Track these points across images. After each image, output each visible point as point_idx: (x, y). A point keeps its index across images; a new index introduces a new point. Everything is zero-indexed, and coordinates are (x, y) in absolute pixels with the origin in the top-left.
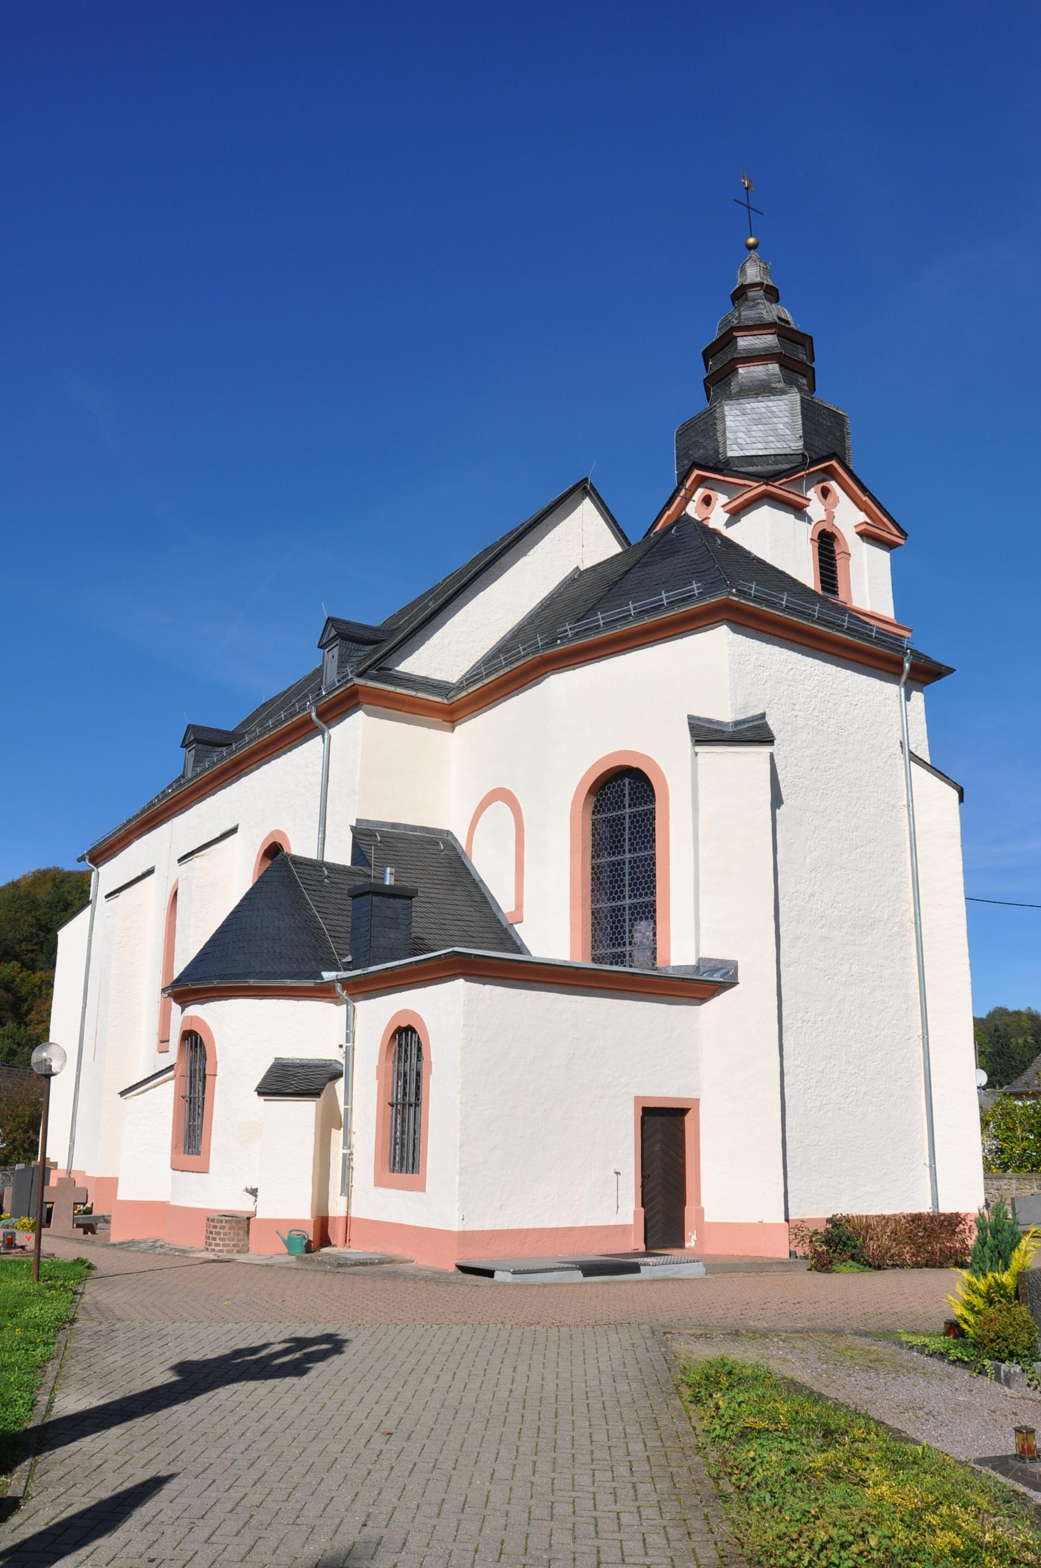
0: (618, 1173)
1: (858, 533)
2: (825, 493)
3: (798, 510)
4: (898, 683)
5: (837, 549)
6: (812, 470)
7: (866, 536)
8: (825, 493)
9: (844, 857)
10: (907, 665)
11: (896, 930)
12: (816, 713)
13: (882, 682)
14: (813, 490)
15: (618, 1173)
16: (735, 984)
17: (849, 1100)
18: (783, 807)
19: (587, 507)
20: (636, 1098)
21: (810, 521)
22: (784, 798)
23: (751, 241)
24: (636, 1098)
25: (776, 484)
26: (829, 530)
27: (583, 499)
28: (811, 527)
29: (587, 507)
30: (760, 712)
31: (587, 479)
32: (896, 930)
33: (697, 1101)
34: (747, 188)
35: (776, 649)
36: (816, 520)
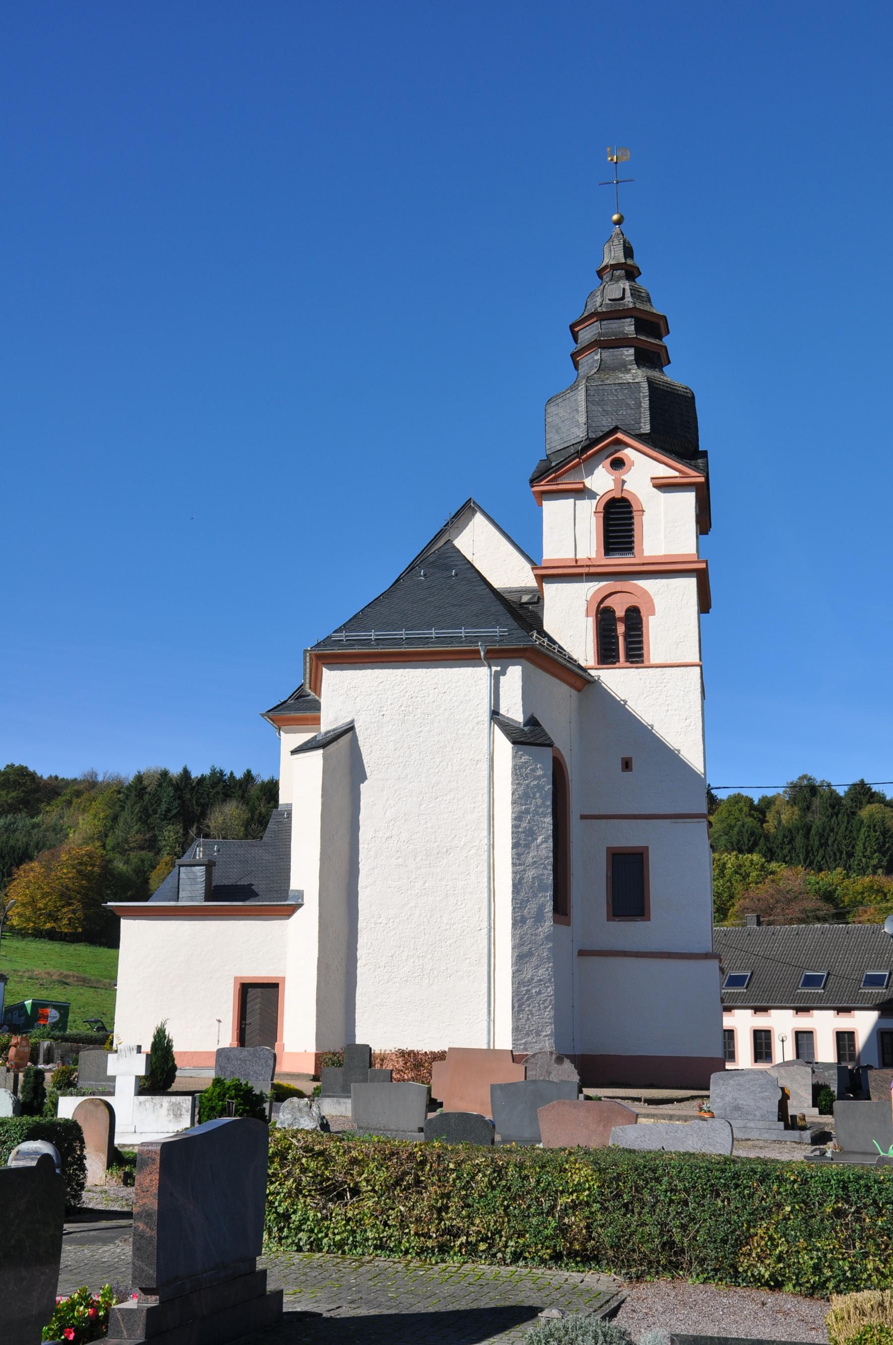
0: (219, 1021)
2: (618, 464)
3: (582, 493)
4: (484, 666)
5: (635, 508)
7: (664, 486)
8: (618, 464)
9: (423, 806)
10: (482, 653)
11: (473, 851)
12: (403, 708)
14: (601, 466)
15: (219, 1021)
16: (302, 905)
17: (416, 975)
18: (366, 782)
19: (479, 519)
20: (235, 978)
21: (591, 495)
22: (368, 775)
23: (615, 217)
24: (235, 978)
25: (542, 483)
26: (618, 496)
27: (473, 515)
28: (595, 502)
29: (479, 519)
30: (348, 720)
32: (473, 851)
33: (284, 979)
35: (369, 671)
36: (601, 492)
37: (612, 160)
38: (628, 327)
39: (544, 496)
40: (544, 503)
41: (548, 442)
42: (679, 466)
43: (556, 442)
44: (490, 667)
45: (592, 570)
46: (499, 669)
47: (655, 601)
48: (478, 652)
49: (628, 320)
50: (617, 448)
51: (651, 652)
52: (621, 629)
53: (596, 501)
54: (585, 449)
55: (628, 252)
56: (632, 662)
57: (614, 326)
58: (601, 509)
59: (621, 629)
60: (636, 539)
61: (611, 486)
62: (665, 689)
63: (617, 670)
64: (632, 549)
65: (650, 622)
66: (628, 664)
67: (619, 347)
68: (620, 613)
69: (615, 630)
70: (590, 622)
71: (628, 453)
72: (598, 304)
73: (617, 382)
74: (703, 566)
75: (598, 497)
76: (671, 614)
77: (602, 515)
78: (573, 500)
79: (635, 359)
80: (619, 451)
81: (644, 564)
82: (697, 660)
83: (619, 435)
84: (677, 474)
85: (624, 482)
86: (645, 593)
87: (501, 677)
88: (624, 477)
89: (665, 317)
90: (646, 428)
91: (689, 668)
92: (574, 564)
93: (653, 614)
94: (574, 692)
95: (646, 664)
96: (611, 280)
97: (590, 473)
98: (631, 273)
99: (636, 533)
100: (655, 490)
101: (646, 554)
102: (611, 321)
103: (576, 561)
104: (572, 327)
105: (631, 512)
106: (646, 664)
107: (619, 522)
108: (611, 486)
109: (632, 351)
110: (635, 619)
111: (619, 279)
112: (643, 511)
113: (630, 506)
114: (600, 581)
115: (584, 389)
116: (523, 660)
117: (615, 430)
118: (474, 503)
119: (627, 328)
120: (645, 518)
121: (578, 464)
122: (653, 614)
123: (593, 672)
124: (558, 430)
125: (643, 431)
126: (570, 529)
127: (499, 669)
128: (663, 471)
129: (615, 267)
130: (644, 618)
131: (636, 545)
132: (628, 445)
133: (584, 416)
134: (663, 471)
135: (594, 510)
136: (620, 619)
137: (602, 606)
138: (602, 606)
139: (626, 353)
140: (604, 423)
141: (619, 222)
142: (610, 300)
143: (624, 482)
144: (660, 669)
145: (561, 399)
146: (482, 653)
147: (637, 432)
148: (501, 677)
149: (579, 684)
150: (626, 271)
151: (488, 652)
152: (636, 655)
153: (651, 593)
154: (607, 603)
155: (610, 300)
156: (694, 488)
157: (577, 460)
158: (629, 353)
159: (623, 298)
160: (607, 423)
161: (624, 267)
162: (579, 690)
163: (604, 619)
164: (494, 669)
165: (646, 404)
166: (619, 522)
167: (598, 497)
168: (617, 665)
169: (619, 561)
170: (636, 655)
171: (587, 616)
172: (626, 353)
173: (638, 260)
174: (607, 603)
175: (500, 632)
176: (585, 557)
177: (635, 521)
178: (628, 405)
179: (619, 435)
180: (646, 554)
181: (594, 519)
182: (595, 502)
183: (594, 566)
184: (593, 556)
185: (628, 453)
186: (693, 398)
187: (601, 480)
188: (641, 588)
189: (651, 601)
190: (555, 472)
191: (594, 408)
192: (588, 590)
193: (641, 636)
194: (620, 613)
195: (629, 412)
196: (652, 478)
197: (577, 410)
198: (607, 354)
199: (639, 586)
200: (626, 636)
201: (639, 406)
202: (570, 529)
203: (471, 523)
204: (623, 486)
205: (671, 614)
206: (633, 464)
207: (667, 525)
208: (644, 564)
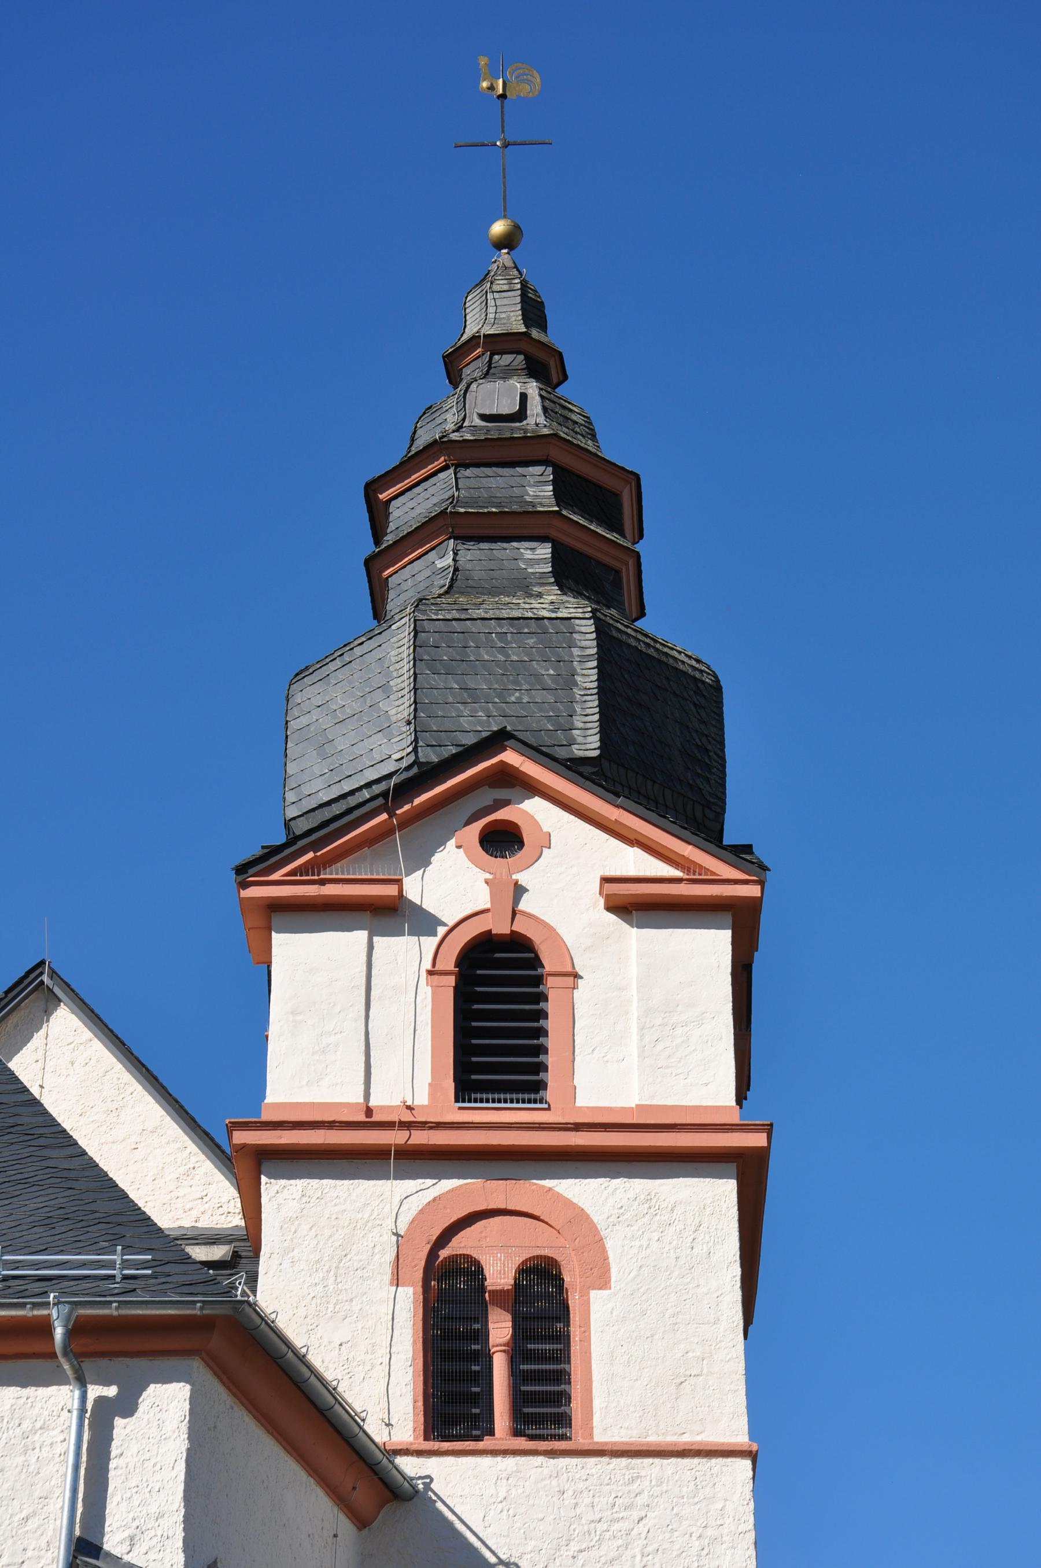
1: (609, 908)
2: (502, 840)
3: (390, 914)
4: (59, 1380)
6: (417, 801)
7: (635, 905)
8: (502, 840)
10: (59, 1332)
13: (30, 1391)
14: (451, 844)
21: (422, 922)
23: (498, 228)
25: (276, 876)
26: (501, 928)
27: (48, 1013)
28: (430, 943)
31: (42, 963)
34: (503, 96)
37: (491, 88)
38: (537, 488)
39: (276, 919)
40: (274, 935)
41: (291, 783)
42: (687, 850)
43: (314, 781)
44: (82, 1382)
45: (420, 1138)
46: (112, 1391)
47: (609, 1245)
48: (44, 1328)
49: (538, 470)
50: (501, 794)
51: (597, 1403)
52: (500, 1329)
53: (436, 940)
54: (406, 789)
55: (533, 310)
56: (532, 1438)
57: (492, 483)
58: (448, 962)
59: (500, 1329)
60: (551, 1060)
61: (482, 899)
62: (642, 1528)
63: (486, 1461)
64: (540, 1086)
65: (594, 1308)
66: (522, 1443)
67: (508, 539)
68: (500, 1273)
69: (483, 1335)
70: (407, 1301)
71: (535, 811)
72: (450, 426)
73: (505, 614)
74: (758, 1140)
75: (441, 931)
76: (660, 1288)
77: (451, 980)
78: (361, 936)
79: (555, 573)
80: (506, 803)
81: (578, 1127)
82: (738, 1434)
83: (510, 757)
84: (677, 873)
85: (519, 890)
86: (580, 1217)
87: (119, 1422)
88: (523, 878)
89: (637, 477)
90: (588, 743)
91: (717, 1462)
92: (362, 1118)
93: (604, 1283)
94: (345, 1526)
95: (579, 1441)
96: (486, 375)
97: (421, 861)
98: (545, 366)
99: (553, 1042)
100: (611, 917)
101: (579, 1103)
102: (488, 471)
103: (369, 1112)
104: (371, 489)
105: (538, 980)
106: (579, 1441)
107: (501, 1004)
108: (482, 899)
109: (545, 551)
110: (543, 1300)
111: (508, 373)
112: (576, 976)
113: (536, 962)
114: (440, 1177)
115: (409, 629)
116: (196, 1365)
117: (499, 740)
118: (53, 974)
119: (531, 491)
120: (582, 995)
121: (384, 834)
122: (604, 1283)
123: (409, 1466)
124: (323, 745)
125: (577, 752)
126: (350, 1018)
127: (112, 1391)
128: (634, 862)
129: (497, 343)
130: (574, 1300)
131: (551, 1077)
132: (533, 788)
133: (408, 700)
134: (634, 862)
135: (427, 964)
136: (499, 1297)
137: (444, 1253)
138: (444, 1253)
139: (528, 555)
140: (465, 723)
141: (507, 242)
142: (483, 417)
143: (519, 890)
144: (624, 1461)
145: (338, 663)
146: (59, 1332)
147: (561, 753)
148: (119, 1422)
149: (363, 1496)
150: (528, 358)
151: (77, 1330)
152: (546, 1413)
153: (598, 1218)
154: (461, 1244)
155: (483, 417)
156: (728, 918)
157: (384, 816)
158: (537, 556)
159: (521, 414)
160: (473, 723)
161: (523, 345)
162: (361, 1522)
163: (450, 1298)
164: (95, 1391)
165: (588, 677)
166: (501, 1004)
167: (441, 931)
168: (487, 1443)
169: (500, 1121)
170: (546, 1413)
171: (397, 1282)
172: (528, 555)
173: (557, 334)
174: (461, 1244)
175: (126, 1264)
176: (396, 1102)
177: (551, 1007)
178: (538, 677)
179: (510, 757)
180: (579, 1103)
181: (426, 992)
182: (430, 943)
183: (423, 1125)
184: (422, 1099)
185: (535, 811)
186: (717, 688)
187: (452, 883)
188: (568, 1203)
189: (599, 1243)
190: (315, 846)
191: (437, 680)
192: (397, 1205)
193: (564, 1356)
194: (500, 1273)
195: (539, 696)
196: (606, 880)
197: (385, 688)
198: (472, 555)
199: (559, 1196)
200: (517, 1353)
201: (569, 682)
202: (350, 1018)
203: (38, 1039)
204: (517, 899)
205: (660, 1288)
206: (546, 841)
207: (647, 1020)
208: (578, 1127)
